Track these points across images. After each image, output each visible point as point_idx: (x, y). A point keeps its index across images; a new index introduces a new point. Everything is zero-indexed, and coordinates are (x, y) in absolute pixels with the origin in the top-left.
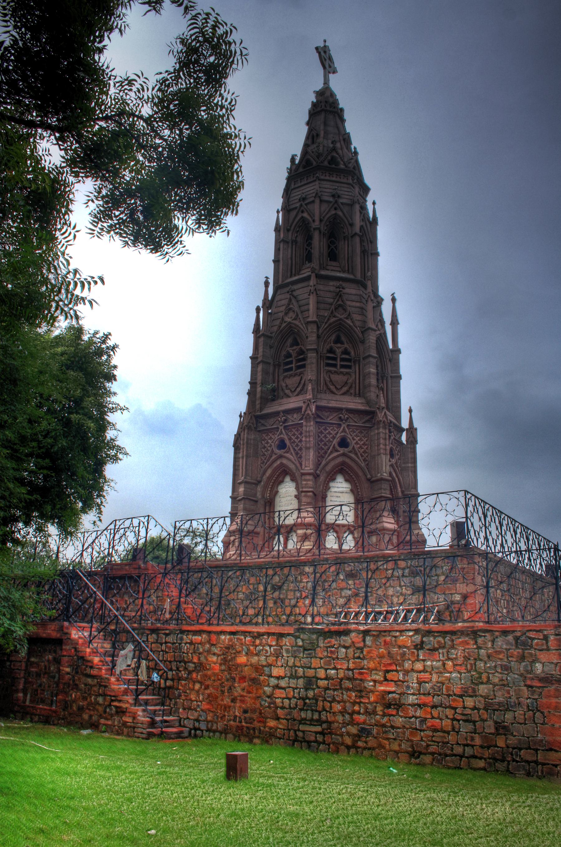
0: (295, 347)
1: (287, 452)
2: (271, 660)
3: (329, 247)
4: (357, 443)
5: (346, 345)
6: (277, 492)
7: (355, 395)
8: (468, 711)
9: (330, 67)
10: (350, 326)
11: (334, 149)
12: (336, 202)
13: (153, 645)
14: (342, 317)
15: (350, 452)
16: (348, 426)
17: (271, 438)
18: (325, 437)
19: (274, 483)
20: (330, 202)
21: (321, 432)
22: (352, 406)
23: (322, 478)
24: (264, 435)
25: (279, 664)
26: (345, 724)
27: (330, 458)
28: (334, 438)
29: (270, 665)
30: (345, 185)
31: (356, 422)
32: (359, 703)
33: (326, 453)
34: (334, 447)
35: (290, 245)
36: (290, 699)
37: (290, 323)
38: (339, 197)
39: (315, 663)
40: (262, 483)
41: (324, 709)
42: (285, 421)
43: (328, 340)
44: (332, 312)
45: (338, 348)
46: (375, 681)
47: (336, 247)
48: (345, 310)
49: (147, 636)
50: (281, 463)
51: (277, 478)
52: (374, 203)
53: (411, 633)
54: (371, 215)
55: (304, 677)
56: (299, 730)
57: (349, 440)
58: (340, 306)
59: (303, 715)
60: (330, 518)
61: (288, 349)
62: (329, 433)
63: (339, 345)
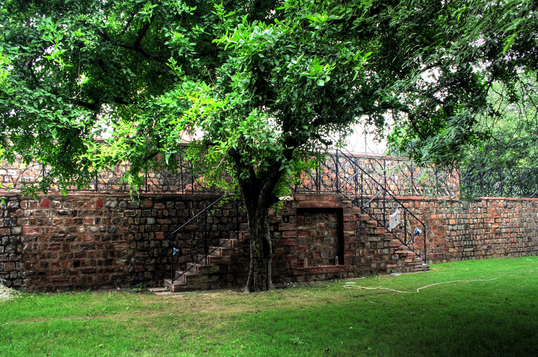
2: (448, 215)
8: (521, 234)
13: (375, 210)
25: (453, 217)
26: (482, 245)
29: (448, 219)
32: (487, 234)
36: (459, 236)
39: (469, 216)
41: (474, 239)
46: (491, 223)
49: (370, 204)
53: (502, 201)
55: (464, 224)
56: (464, 251)
59: (465, 243)
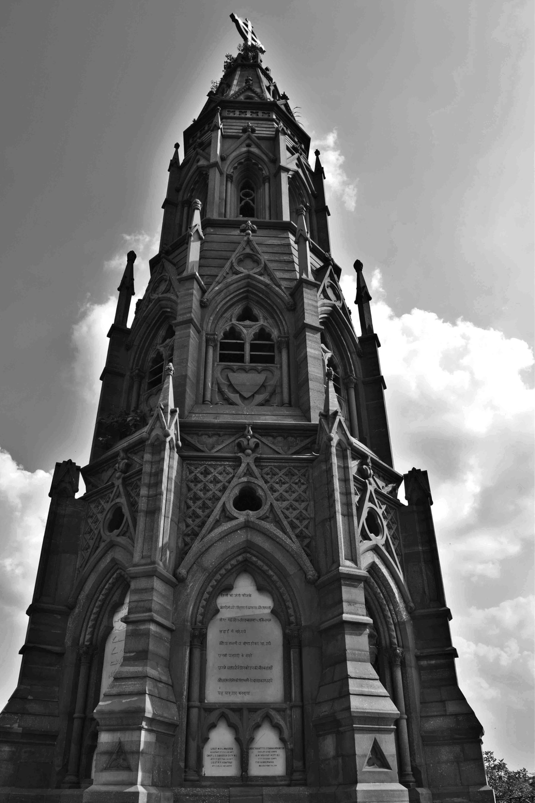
0: (168, 341)
1: (123, 535)
3: (242, 200)
4: (281, 498)
5: (261, 322)
6: (112, 628)
7: (282, 404)
9: (253, 39)
10: (267, 285)
11: (249, 88)
12: (249, 137)
14: (251, 273)
15: (264, 518)
16: (257, 460)
17: (102, 512)
18: (205, 489)
19: (101, 607)
20: (237, 137)
21: (196, 481)
22: (268, 418)
23: (193, 586)
24: (92, 506)
27: (213, 534)
28: (224, 489)
30: (264, 122)
31: (278, 453)
33: (203, 523)
34: (224, 509)
35: (179, 207)
37: (159, 300)
38: (253, 131)
40: (77, 610)
42: (128, 466)
43: (227, 315)
44: (232, 267)
45: (245, 327)
47: (253, 200)
48: (257, 262)
50: (113, 560)
51: (107, 595)
52: (317, 153)
54: (313, 168)
57: (260, 492)
58: (248, 256)
60: (214, 694)
61: (158, 347)
62: (216, 481)
63: (247, 322)
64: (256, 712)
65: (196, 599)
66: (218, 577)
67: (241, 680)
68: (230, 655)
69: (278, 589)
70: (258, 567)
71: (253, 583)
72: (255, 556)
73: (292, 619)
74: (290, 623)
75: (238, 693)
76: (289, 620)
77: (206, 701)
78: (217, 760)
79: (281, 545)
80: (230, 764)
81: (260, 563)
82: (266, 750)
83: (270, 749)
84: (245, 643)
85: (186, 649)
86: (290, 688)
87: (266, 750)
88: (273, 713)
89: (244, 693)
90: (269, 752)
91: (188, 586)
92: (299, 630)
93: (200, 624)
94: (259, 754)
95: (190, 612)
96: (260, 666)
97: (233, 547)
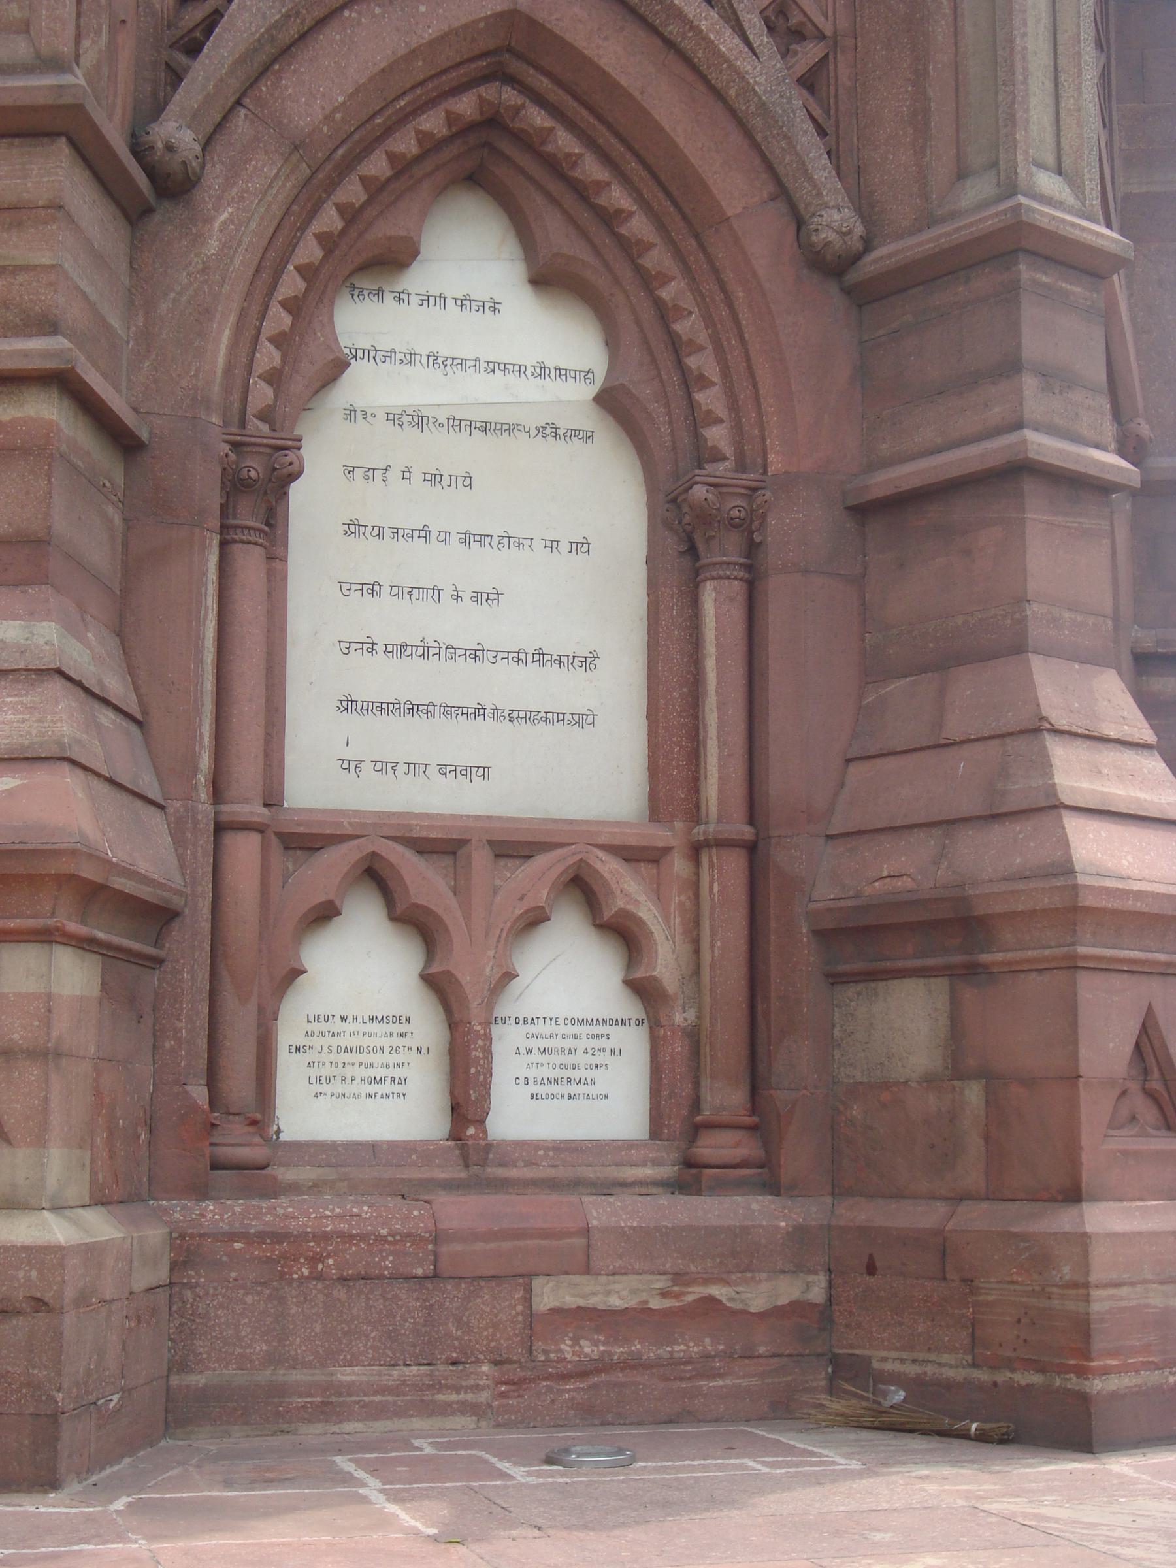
64: (529, 857)
65: (248, 295)
66: (352, 191)
67: (447, 710)
68: (398, 591)
69: (648, 281)
70: (555, 166)
71: (512, 248)
72: (540, 100)
73: (717, 435)
74: (704, 455)
75: (433, 770)
76: (696, 435)
77: (286, 805)
78: (339, 1071)
79: (685, 58)
80: (397, 1088)
81: (564, 141)
82: (561, 1029)
83: (581, 1022)
84: (468, 538)
85: (204, 547)
86: (695, 755)
87: (561, 1029)
88: (608, 867)
89: (465, 770)
90: (577, 1037)
91: (209, 220)
92: (755, 489)
93: (265, 428)
94: (535, 1044)
95: (221, 361)
96: (540, 652)
97: (442, 39)
